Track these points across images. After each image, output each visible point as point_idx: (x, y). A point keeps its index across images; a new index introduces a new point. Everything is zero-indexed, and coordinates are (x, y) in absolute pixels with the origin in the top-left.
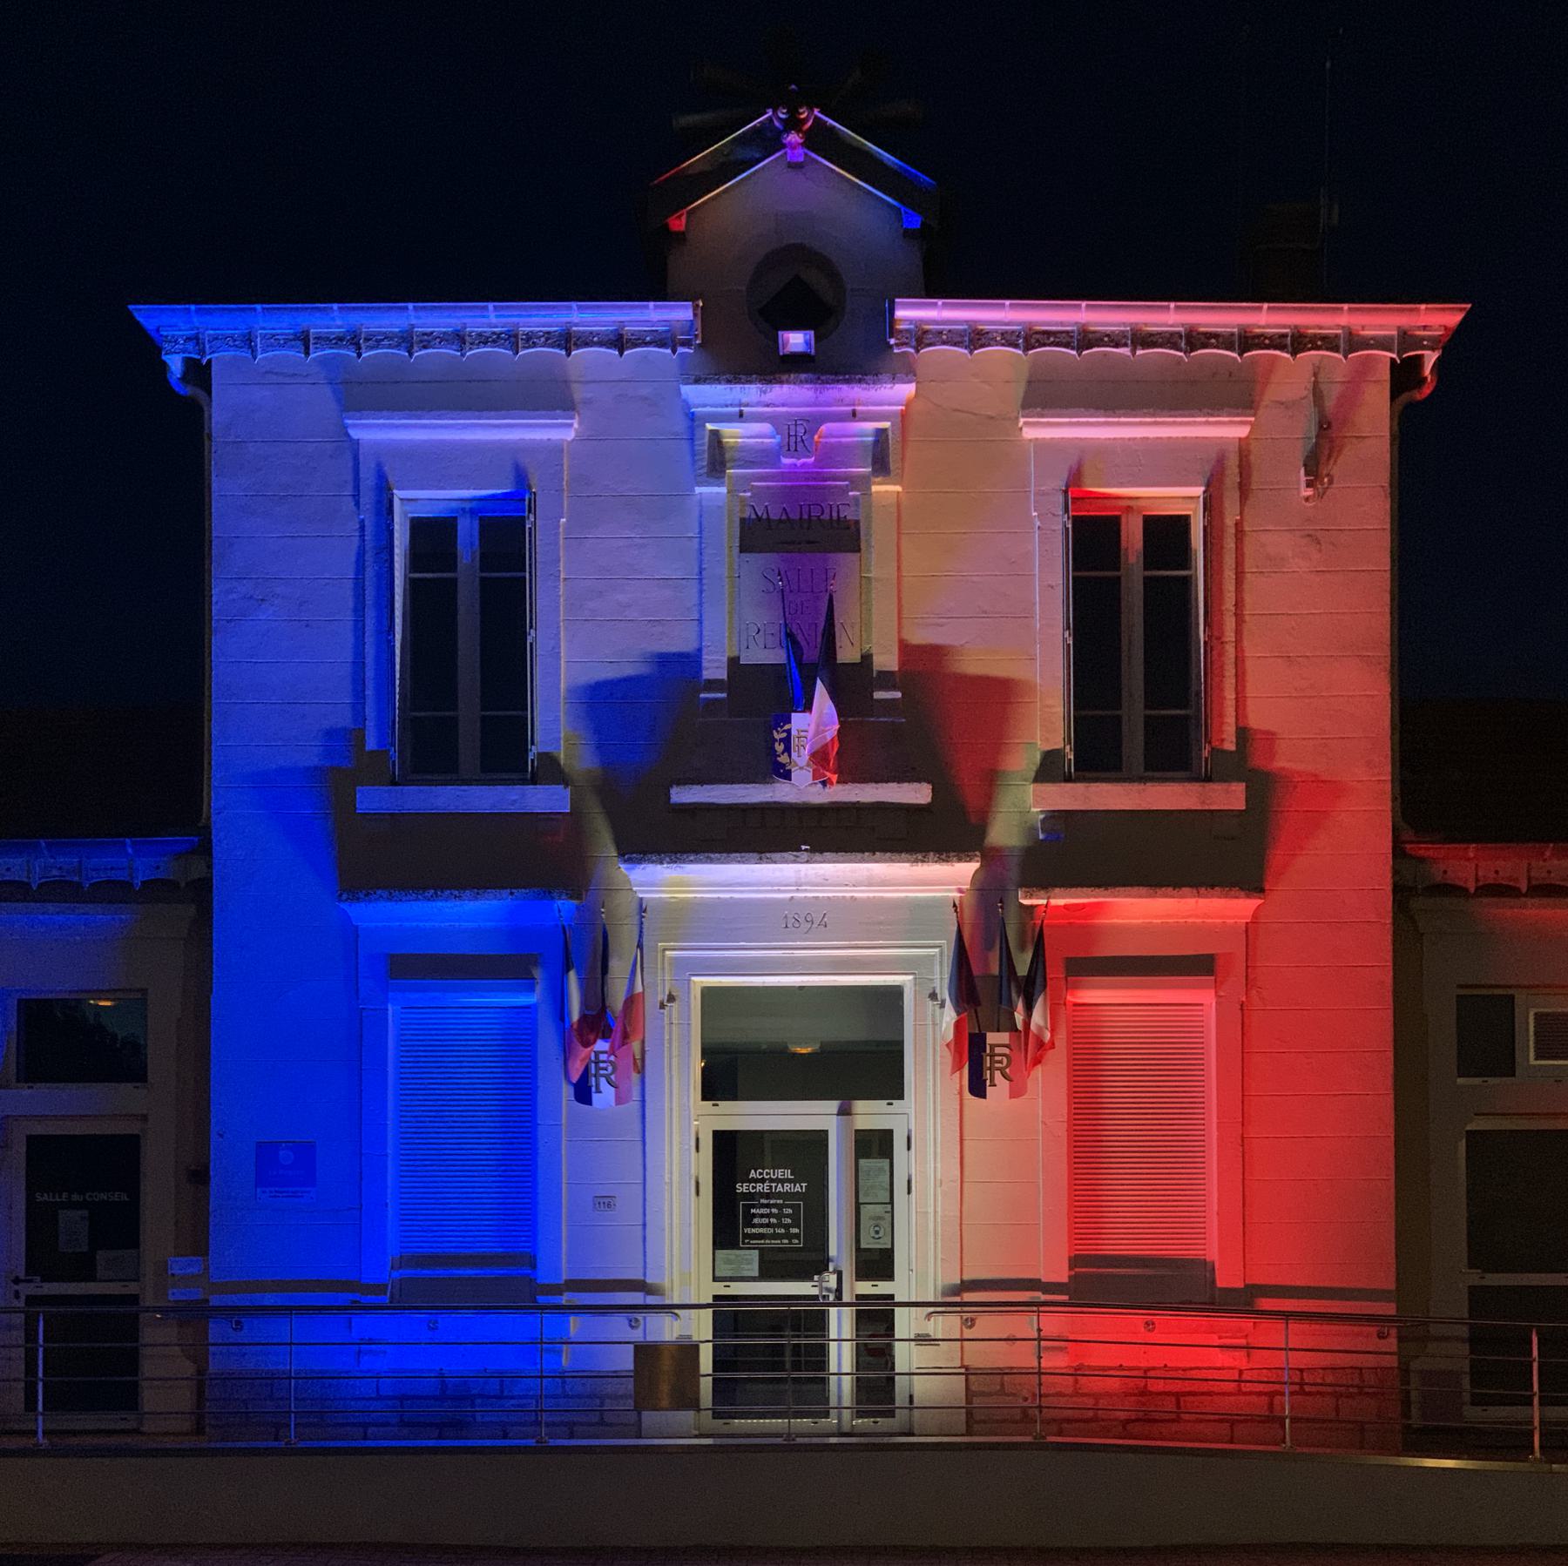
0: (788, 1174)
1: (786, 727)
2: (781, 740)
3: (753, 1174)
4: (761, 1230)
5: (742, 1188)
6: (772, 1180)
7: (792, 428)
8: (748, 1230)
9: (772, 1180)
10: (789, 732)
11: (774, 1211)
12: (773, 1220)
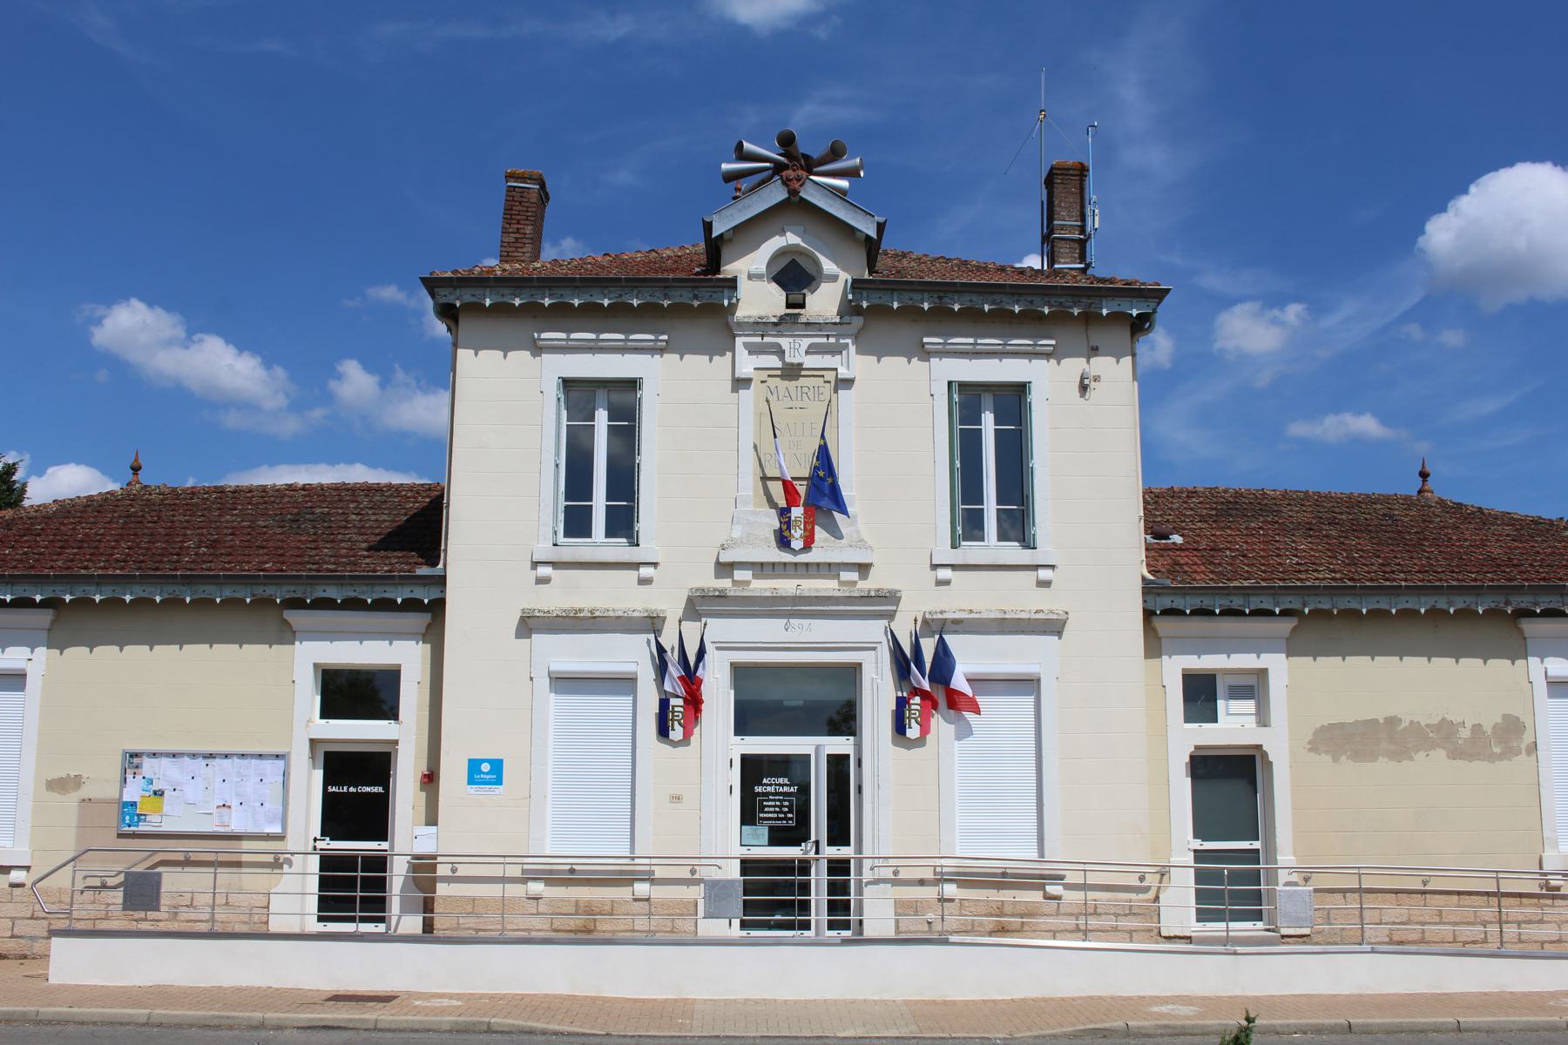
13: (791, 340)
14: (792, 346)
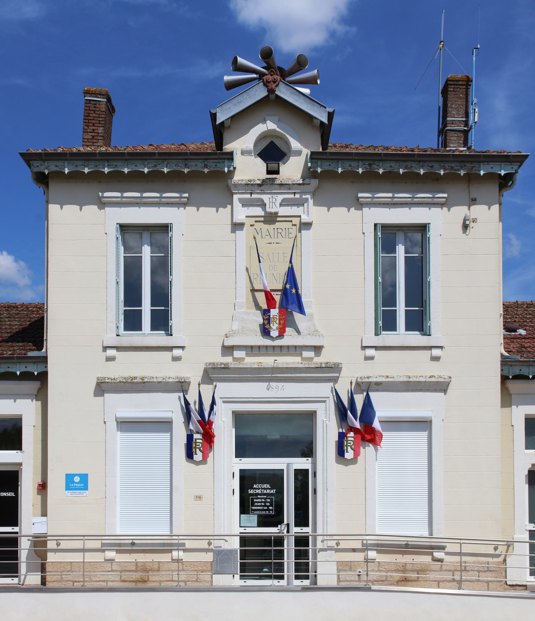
0: (268, 486)
1: (268, 314)
2: (266, 319)
3: (255, 486)
4: (258, 508)
5: (251, 491)
6: (262, 489)
7: (271, 199)
8: (253, 508)
9: (262, 489)
10: (269, 316)
11: (263, 500)
12: (263, 504)
13: (270, 196)
14: (271, 201)
